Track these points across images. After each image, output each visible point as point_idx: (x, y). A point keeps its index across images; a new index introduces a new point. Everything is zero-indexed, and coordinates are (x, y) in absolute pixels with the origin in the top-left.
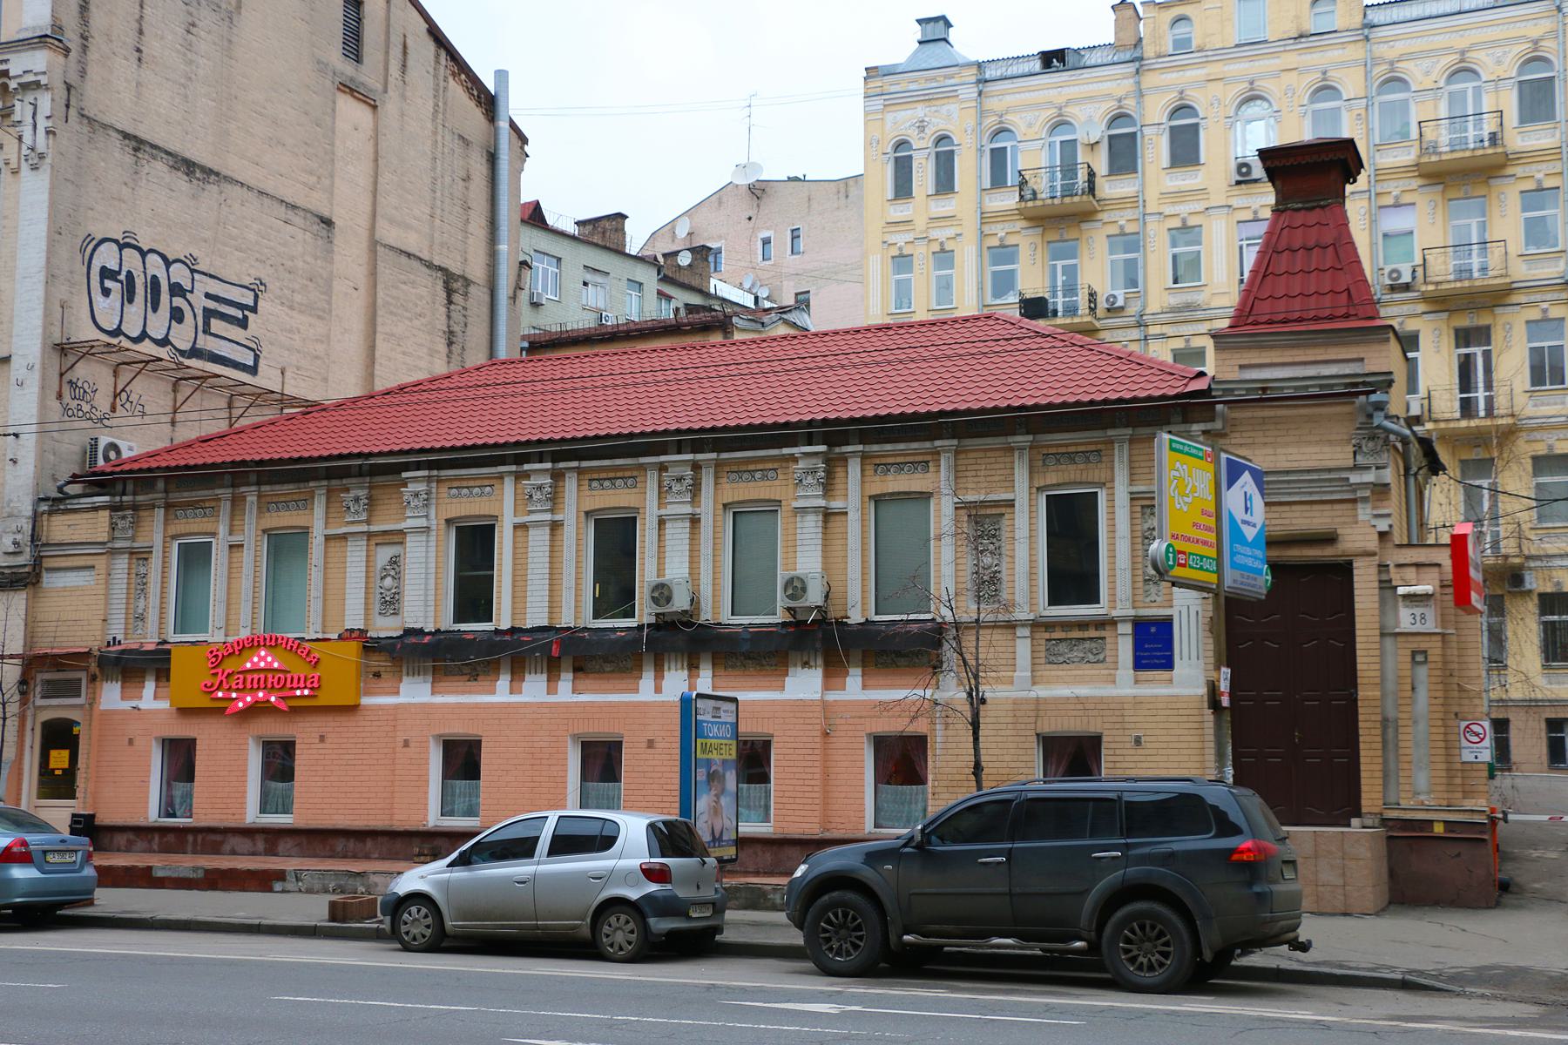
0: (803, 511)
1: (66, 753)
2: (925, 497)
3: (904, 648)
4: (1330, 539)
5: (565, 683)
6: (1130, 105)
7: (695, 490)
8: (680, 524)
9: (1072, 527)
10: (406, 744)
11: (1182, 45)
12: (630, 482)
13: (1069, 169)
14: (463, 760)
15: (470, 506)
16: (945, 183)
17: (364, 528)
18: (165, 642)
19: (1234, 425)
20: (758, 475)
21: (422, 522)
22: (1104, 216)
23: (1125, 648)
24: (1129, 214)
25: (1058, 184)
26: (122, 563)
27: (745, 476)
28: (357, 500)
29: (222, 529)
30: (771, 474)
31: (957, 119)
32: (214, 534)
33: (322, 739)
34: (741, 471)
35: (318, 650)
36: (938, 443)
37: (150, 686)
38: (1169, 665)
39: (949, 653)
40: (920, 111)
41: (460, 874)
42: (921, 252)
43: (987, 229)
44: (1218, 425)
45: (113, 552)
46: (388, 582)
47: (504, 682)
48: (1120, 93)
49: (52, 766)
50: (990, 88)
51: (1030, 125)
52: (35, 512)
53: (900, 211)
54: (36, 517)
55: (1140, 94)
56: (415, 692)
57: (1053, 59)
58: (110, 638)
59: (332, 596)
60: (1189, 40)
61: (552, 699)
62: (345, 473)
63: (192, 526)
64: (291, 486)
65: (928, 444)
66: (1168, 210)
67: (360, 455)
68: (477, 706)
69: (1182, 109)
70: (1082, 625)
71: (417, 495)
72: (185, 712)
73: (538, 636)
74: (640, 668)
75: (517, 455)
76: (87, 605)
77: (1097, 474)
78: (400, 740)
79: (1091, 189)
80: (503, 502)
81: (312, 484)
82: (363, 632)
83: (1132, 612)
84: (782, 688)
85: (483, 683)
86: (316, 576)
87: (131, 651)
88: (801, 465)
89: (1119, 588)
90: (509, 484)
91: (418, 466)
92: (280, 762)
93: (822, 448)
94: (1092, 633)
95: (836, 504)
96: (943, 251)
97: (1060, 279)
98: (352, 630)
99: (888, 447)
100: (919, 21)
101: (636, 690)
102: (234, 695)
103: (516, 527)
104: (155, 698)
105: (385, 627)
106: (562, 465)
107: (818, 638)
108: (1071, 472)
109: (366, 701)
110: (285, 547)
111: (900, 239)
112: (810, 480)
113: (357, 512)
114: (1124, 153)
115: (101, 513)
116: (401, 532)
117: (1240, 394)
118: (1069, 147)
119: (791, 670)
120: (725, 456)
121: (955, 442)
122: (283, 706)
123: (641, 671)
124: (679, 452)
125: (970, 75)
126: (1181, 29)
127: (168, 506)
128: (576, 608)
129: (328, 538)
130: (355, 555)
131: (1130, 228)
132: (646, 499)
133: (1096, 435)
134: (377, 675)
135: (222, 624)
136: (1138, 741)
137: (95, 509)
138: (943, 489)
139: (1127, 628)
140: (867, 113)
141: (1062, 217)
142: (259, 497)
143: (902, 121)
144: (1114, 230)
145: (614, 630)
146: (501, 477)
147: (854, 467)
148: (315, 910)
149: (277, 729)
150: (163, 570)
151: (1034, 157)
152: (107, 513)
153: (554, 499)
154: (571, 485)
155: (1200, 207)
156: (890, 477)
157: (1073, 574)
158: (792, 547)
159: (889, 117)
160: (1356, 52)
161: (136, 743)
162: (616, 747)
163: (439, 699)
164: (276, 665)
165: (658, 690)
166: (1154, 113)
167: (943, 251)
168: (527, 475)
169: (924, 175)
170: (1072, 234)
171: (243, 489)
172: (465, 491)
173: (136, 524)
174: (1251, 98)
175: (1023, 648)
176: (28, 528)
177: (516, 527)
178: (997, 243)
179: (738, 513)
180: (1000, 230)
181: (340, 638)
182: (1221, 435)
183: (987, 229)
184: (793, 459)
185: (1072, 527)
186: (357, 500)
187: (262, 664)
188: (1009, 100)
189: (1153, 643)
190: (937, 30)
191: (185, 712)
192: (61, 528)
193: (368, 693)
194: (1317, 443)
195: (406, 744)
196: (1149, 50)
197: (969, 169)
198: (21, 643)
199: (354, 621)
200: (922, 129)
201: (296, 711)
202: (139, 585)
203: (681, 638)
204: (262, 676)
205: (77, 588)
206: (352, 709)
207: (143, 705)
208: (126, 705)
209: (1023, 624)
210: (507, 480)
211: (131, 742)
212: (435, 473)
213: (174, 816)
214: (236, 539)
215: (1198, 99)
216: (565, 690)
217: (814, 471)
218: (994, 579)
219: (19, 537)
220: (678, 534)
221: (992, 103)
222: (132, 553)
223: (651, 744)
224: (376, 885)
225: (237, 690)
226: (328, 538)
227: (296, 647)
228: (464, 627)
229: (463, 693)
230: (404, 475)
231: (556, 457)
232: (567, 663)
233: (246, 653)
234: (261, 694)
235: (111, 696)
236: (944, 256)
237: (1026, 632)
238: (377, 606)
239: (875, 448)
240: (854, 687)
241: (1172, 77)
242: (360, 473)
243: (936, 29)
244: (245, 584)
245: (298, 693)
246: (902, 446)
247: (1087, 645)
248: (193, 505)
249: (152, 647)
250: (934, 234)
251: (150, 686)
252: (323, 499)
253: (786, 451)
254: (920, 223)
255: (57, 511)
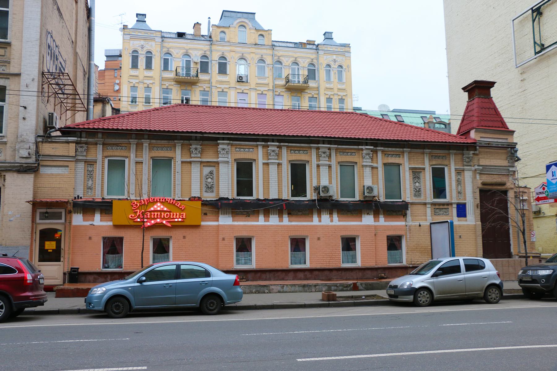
0: (366, 166)
1: (54, 243)
2: (399, 165)
3: (398, 210)
4: (504, 184)
5: (286, 219)
6: (208, 53)
7: (330, 157)
8: (325, 167)
9: (438, 175)
10: (224, 239)
11: (222, 39)
12: (305, 152)
13: (188, 68)
14: (298, 244)
15: (244, 155)
16: (149, 65)
17: (200, 160)
18: (103, 199)
19: (480, 152)
20: (349, 154)
21: (226, 159)
22: (199, 84)
23: (455, 211)
24: (207, 85)
25: (184, 72)
26: (81, 165)
27: (345, 154)
28: (196, 149)
29: (132, 156)
30: (353, 154)
31: (154, 47)
32: (127, 157)
33: (184, 237)
34: (343, 152)
35: (183, 205)
36: (405, 149)
37: (97, 216)
38: (465, 216)
39: (409, 212)
40: (142, 42)
41: (435, 280)
42: (141, 86)
43: (163, 83)
44: (477, 152)
45: (77, 161)
46: (209, 180)
47: (261, 217)
48: (205, 50)
49: (46, 247)
50: (165, 40)
51: (177, 53)
52: (36, 141)
53: (134, 72)
54: (37, 143)
55: (211, 51)
56: (225, 220)
57: (181, 35)
58: (76, 196)
59: (186, 184)
60: (224, 39)
61: (281, 224)
62: (189, 139)
63: (117, 153)
64: (166, 141)
65: (401, 149)
66: (218, 86)
67: (201, 133)
68: (253, 226)
69: (223, 57)
70: (443, 204)
71: (223, 149)
72: (116, 227)
73: (275, 202)
74: (312, 214)
75: (265, 139)
76: (65, 180)
77: (446, 162)
78: (221, 237)
79: (197, 76)
80: (258, 155)
81: (175, 141)
82: (199, 199)
83: (457, 201)
84: (361, 221)
85: (252, 217)
86: (178, 177)
87: (89, 202)
88: (364, 152)
89: (451, 195)
90: (260, 149)
91: (223, 139)
92: (161, 248)
93: (372, 147)
94: (446, 207)
95: (375, 165)
96: (148, 87)
97: (185, 101)
98: (195, 197)
99: (390, 149)
100: (137, 15)
101: (312, 221)
102: (145, 220)
103: (264, 164)
104: (101, 221)
105: (210, 196)
106: (282, 144)
107: (369, 205)
108: (439, 161)
109: (203, 223)
110: (161, 164)
111: (134, 81)
112: (367, 157)
113: (196, 154)
114: (204, 67)
115: (70, 144)
116: (218, 163)
117: (483, 145)
118: (188, 62)
119: (363, 216)
120: (339, 146)
121: (409, 150)
122: (169, 225)
123: (259, 214)
124: (324, 144)
125: (159, 35)
126: (223, 35)
127: (104, 144)
128: (286, 194)
129: (182, 162)
130: (195, 170)
131: (207, 89)
132: (311, 158)
133: (447, 152)
134: (205, 214)
135: (134, 192)
136: (460, 237)
137: (68, 142)
138: (406, 163)
139: (455, 206)
140: (124, 39)
141: (186, 83)
142: (149, 144)
143: (136, 44)
144: (202, 89)
145: (299, 201)
146: (257, 146)
147: (380, 154)
148: (316, 297)
149: (161, 234)
150: (101, 169)
151: (177, 63)
152: (74, 145)
153: (279, 156)
154: (284, 150)
155: (227, 86)
156: (389, 158)
157: (439, 190)
158: (362, 177)
159: (132, 42)
160: (270, 52)
161: (93, 239)
162: (249, 240)
163: (236, 223)
164: (165, 209)
165: (320, 221)
166: (215, 57)
167: (148, 87)
168: (268, 146)
169: (142, 62)
170: (189, 88)
171: (143, 141)
172: (242, 150)
173: (87, 150)
174: (242, 58)
175: (429, 210)
176: (33, 147)
177: (264, 164)
178: (166, 87)
179: (342, 165)
180: (167, 84)
181: (190, 200)
182: (477, 155)
183: (163, 83)
184: (362, 150)
185: (438, 175)
186: (196, 149)
187: (159, 209)
188: (171, 45)
189: (462, 211)
190: (141, 18)
191: (116, 227)
192: (47, 149)
193: (203, 221)
194: (500, 159)
195: (224, 239)
196: (214, 38)
197: (157, 63)
198: (32, 196)
199: (196, 193)
200: (142, 48)
201: (173, 227)
202: (90, 175)
203: (325, 204)
204: (159, 213)
205: (59, 175)
206: (197, 226)
207: (95, 223)
208: (87, 223)
209: (429, 203)
210: (259, 147)
211: (90, 238)
212: (232, 142)
213: (108, 267)
214: (139, 160)
215: (227, 55)
216: (286, 221)
217: (368, 154)
218: (419, 191)
219: (30, 151)
220: (324, 171)
221: (165, 44)
222: (86, 162)
223: (319, 239)
224: (273, 289)
225: (147, 218)
226: (182, 162)
227: (173, 203)
228: (241, 198)
229: (245, 221)
230: (219, 142)
231: (279, 141)
232: (285, 212)
233: (150, 205)
234: (158, 220)
235: (78, 219)
236: (148, 88)
237: (430, 206)
238: (204, 189)
239: (386, 149)
240: (382, 221)
241: (220, 48)
242: (196, 139)
243: (141, 18)
244: (145, 178)
245: (176, 220)
246: (394, 149)
247: (444, 210)
248: (117, 145)
249: (100, 200)
250: (145, 81)
251: (97, 216)
252: (180, 147)
253: (360, 147)
254: (141, 77)
255: (46, 142)
